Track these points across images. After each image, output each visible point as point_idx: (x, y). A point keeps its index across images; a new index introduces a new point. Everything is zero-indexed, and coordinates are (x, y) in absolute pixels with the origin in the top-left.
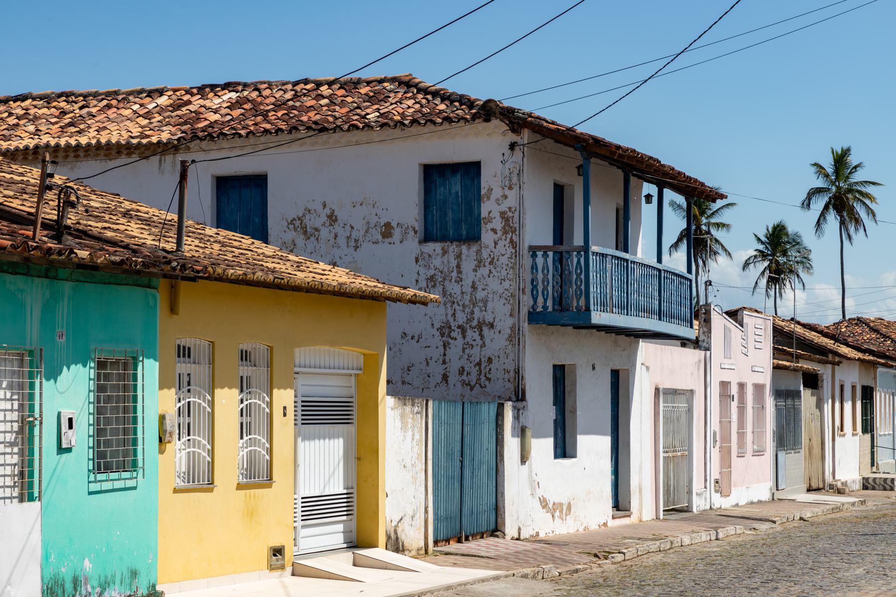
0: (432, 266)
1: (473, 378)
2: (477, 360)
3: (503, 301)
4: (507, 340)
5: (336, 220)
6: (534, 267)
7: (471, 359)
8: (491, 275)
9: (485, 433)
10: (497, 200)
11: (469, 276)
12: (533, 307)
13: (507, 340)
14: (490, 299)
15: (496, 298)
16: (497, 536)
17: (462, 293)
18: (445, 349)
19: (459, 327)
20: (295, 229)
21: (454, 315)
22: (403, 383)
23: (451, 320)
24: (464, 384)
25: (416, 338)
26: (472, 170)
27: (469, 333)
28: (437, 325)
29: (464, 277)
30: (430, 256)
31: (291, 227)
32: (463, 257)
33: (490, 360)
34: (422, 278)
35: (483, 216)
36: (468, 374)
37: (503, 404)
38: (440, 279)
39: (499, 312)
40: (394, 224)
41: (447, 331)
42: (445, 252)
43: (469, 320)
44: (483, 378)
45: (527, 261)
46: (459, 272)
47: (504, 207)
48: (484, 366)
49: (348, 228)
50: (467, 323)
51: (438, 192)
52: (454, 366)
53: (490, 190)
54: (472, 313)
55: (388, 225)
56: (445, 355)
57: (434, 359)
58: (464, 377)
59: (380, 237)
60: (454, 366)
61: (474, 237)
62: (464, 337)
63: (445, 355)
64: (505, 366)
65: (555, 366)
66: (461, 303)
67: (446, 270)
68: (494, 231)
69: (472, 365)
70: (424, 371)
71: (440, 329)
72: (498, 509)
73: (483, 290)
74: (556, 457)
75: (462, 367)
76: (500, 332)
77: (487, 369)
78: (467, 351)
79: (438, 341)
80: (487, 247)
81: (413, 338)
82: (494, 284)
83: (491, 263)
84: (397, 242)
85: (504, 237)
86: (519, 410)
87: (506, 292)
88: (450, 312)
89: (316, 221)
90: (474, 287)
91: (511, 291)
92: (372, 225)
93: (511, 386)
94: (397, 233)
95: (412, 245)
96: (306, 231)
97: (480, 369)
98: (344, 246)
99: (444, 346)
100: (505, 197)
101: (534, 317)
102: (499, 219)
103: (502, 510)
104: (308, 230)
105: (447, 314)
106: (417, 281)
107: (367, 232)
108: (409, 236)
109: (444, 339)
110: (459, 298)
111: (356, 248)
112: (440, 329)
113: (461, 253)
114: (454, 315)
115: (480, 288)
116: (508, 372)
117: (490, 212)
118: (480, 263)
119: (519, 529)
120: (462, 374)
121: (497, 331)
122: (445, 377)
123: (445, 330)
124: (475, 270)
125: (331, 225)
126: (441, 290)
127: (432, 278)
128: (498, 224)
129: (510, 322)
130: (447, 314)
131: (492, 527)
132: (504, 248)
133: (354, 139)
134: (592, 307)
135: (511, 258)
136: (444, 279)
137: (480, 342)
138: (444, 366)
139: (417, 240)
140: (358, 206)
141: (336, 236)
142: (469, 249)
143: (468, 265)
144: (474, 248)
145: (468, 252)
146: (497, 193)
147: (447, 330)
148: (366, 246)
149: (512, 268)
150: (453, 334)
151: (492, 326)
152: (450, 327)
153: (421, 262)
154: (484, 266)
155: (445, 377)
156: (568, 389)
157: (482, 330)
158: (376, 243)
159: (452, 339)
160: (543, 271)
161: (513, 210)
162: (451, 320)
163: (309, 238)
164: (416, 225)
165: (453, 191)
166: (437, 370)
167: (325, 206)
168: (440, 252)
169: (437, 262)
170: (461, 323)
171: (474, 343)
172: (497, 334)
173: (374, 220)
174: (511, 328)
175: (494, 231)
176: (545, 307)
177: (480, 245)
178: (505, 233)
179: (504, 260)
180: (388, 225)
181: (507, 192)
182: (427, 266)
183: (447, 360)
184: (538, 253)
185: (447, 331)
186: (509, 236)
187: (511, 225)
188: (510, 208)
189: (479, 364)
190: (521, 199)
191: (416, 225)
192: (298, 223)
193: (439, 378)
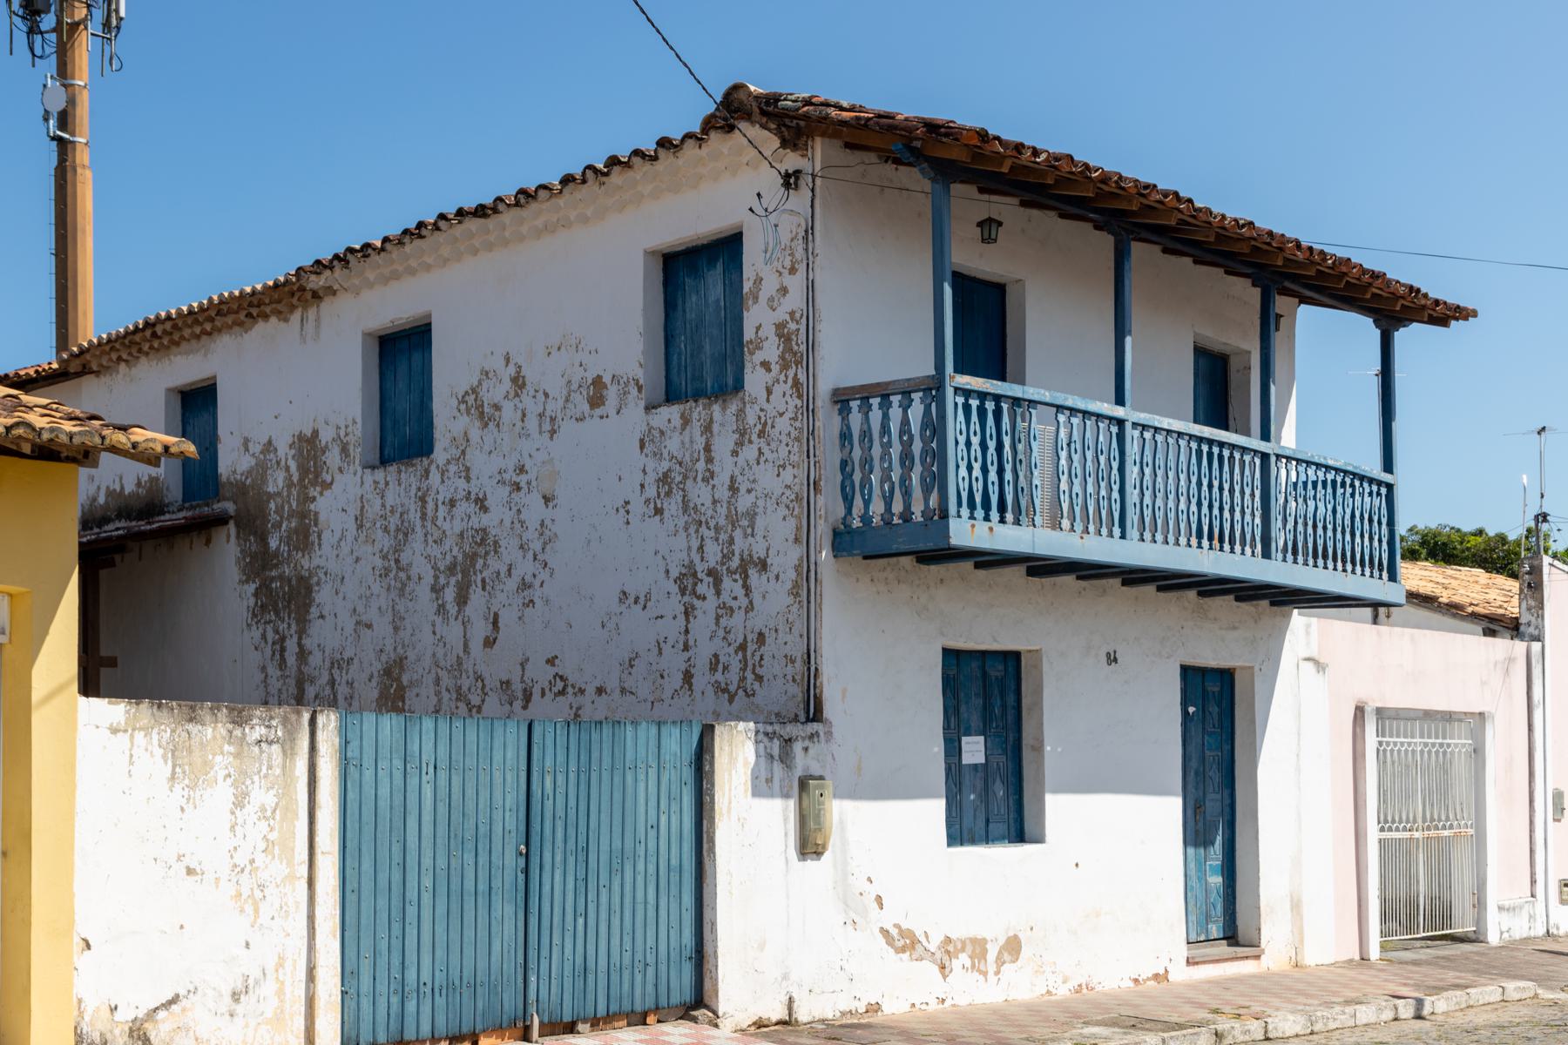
0: (665, 455)
1: (733, 677)
2: (740, 640)
3: (783, 511)
4: (790, 593)
5: (524, 384)
6: (845, 436)
7: (731, 637)
8: (762, 459)
9: (643, 790)
10: (771, 299)
11: (725, 467)
12: (844, 518)
13: (790, 593)
14: (760, 510)
15: (771, 505)
16: (695, 1020)
17: (715, 502)
18: (688, 621)
19: (710, 573)
20: (468, 413)
21: (701, 548)
22: (623, 691)
23: (697, 560)
24: (722, 689)
25: (642, 600)
26: (728, 247)
27: (727, 583)
28: (674, 573)
29: (716, 469)
30: (662, 433)
31: (463, 407)
32: (716, 428)
33: (761, 638)
34: (651, 479)
35: (746, 338)
36: (725, 668)
37: (713, 727)
38: (679, 479)
39: (775, 535)
40: (607, 379)
41: (689, 582)
42: (686, 421)
43: (727, 557)
44: (750, 676)
45: (828, 423)
46: (710, 460)
47: (781, 315)
48: (750, 647)
49: (540, 396)
50: (723, 564)
51: (688, 305)
52: (704, 651)
53: (759, 281)
54: (731, 541)
55: (598, 382)
56: (687, 631)
57: (671, 642)
58: (719, 676)
59: (586, 407)
60: (704, 651)
61: (729, 386)
62: (718, 593)
63: (687, 631)
64: (787, 650)
65: (952, 656)
66: (712, 524)
67: (687, 458)
68: (766, 365)
69: (731, 650)
70: (654, 667)
71: (679, 580)
72: (700, 957)
73: (749, 491)
74: (949, 845)
75: (716, 656)
76: (777, 577)
77: (757, 658)
78: (723, 621)
79: (675, 605)
80: (754, 402)
81: (636, 601)
82: (767, 480)
83: (761, 434)
84: (612, 413)
85: (782, 378)
87: (788, 492)
88: (695, 544)
89: (496, 392)
90: (733, 489)
91: (796, 489)
92: (575, 386)
93: (796, 691)
94: (612, 393)
95: (635, 410)
96: (482, 413)
97: (745, 657)
98: (535, 435)
99: (686, 613)
100: (784, 291)
101: (844, 541)
102: (773, 339)
103: (711, 959)
104: (486, 410)
105: (689, 548)
106: (642, 486)
107: (567, 400)
108: (630, 397)
109: (686, 598)
110: (710, 513)
111: (553, 432)
112: (679, 580)
113: (711, 421)
114: (701, 548)
115: (743, 489)
116: (793, 662)
117: (758, 328)
118: (742, 432)
119: (791, 1000)
120: (716, 670)
121: (772, 576)
122: (688, 677)
123: (687, 581)
124: (735, 453)
125: (517, 395)
126: (680, 500)
127: (665, 479)
128: (771, 351)
129: (796, 553)
130: (689, 548)
131: (688, 996)
132: (784, 401)
133: (539, 222)
134: (952, 509)
135: (795, 419)
136: (685, 477)
137: (744, 602)
138: (686, 655)
139: (642, 404)
140: (554, 351)
141: (524, 415)
142: (724, 409)
143: (723, 443)
144: (733, 407)
145: (722, 415)
146: (769, 287)
147: (691, 580)
148: (567, 428)
149: (797, 439)
150: (701, 589)
151: (763, 565)
152: (695, 575)
153: (649, 449)
154: (750, 442)
155: (688, 677)
156: (1025, 702)
157: (747, 576)
158: (580, 419)
159: (698, 597)
160: (861, 441)
161: (798, 315)
162: (697, 560)
163: (486, 425)
164: (640, 374)
165: (712, 299)
166: (674, 662)
167: (508, 360)
168: (677, 422)
169: (673, 444)
170: (712, 564)
171: (735, 604)
172: (773, 581)
173: (577, 375)
174: (797, 568)
175: (766, 365)
176: (866, 519)
177: (743, 399)
178: (785, 367)
179: (783, 424)
180: (598, 382)
181: (788, 280)
182: (658, 455)
183: (691, 643)
184: (852, 404)
185: (689, 582)
186: (791, 373)
187: (798, 350)
188: (792, 314)
189: (743, 647)
190: (811, 287)
191: (640, 374)
192: (471, 399)
193: (678, 679)
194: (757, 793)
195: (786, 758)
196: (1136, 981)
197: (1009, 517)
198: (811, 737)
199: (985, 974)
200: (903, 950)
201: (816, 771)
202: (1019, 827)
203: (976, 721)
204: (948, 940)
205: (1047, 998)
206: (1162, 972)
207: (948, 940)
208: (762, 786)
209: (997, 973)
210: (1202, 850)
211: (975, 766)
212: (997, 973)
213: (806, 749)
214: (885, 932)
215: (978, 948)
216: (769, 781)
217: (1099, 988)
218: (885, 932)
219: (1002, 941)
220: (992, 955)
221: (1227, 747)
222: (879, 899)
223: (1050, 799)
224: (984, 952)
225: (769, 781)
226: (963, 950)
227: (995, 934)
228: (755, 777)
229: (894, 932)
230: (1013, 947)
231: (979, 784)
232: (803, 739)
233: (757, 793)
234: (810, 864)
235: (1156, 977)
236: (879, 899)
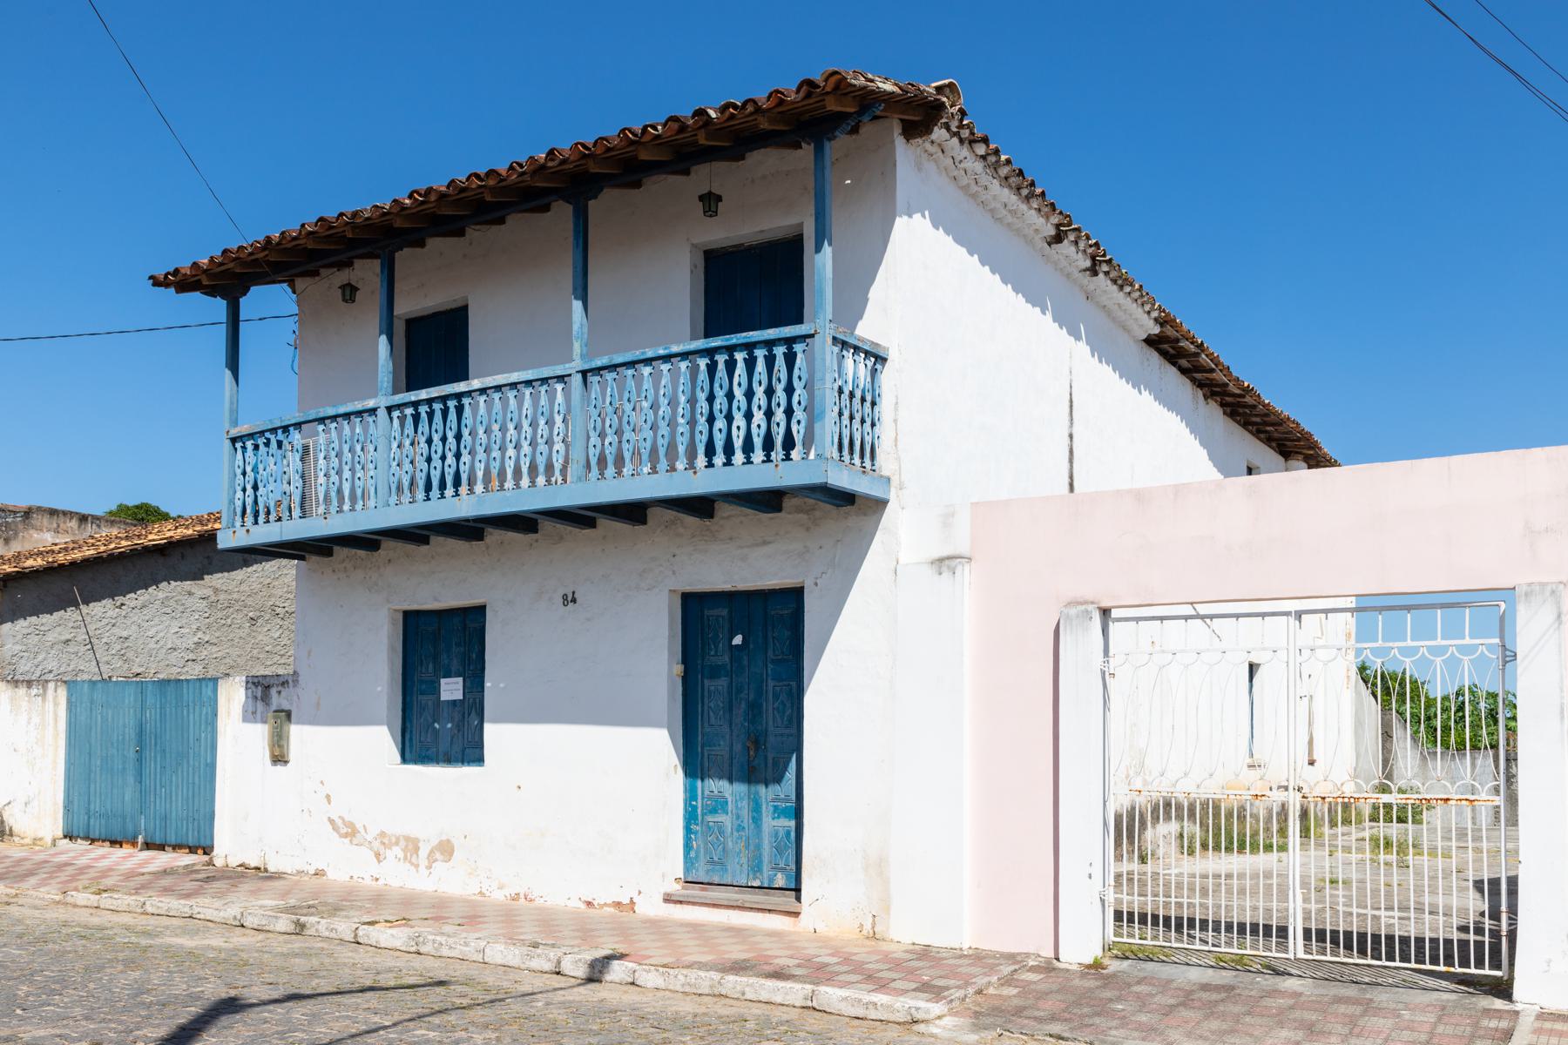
86: (268, 687)
194: (245, 720)
195: (265, 698)
196: (589, 904)
197: (261, 519)
199: (417, 866)
200: (346, 835)
201: (286, 706)
202: (470, 751)
204: (383, 834)
205: (478, 898)
206: (626, 901)
207: (383, 834)
208: (250, 716)
209: (429, 867)
210: (762, 789)
211: (455, 701)
212: (429, 867)
214: (331, 821)
215: (411, 846)
216: (254, 713)
217: (539, 902)
218: (331, 821)
219: (435, 842)
220: (424, 852)
222: (328, 797)
223: (488, 727)
224: (417, 849)
225: (254, 713)
226: (397, 843)
227: (429, 836)
228: (245, 711)
229: (339, 822)
230: (446, 849)
231: (457, 717)
233: (245, 720)
234: (279, 768)
235: (618, 904)
236: (328, 797)
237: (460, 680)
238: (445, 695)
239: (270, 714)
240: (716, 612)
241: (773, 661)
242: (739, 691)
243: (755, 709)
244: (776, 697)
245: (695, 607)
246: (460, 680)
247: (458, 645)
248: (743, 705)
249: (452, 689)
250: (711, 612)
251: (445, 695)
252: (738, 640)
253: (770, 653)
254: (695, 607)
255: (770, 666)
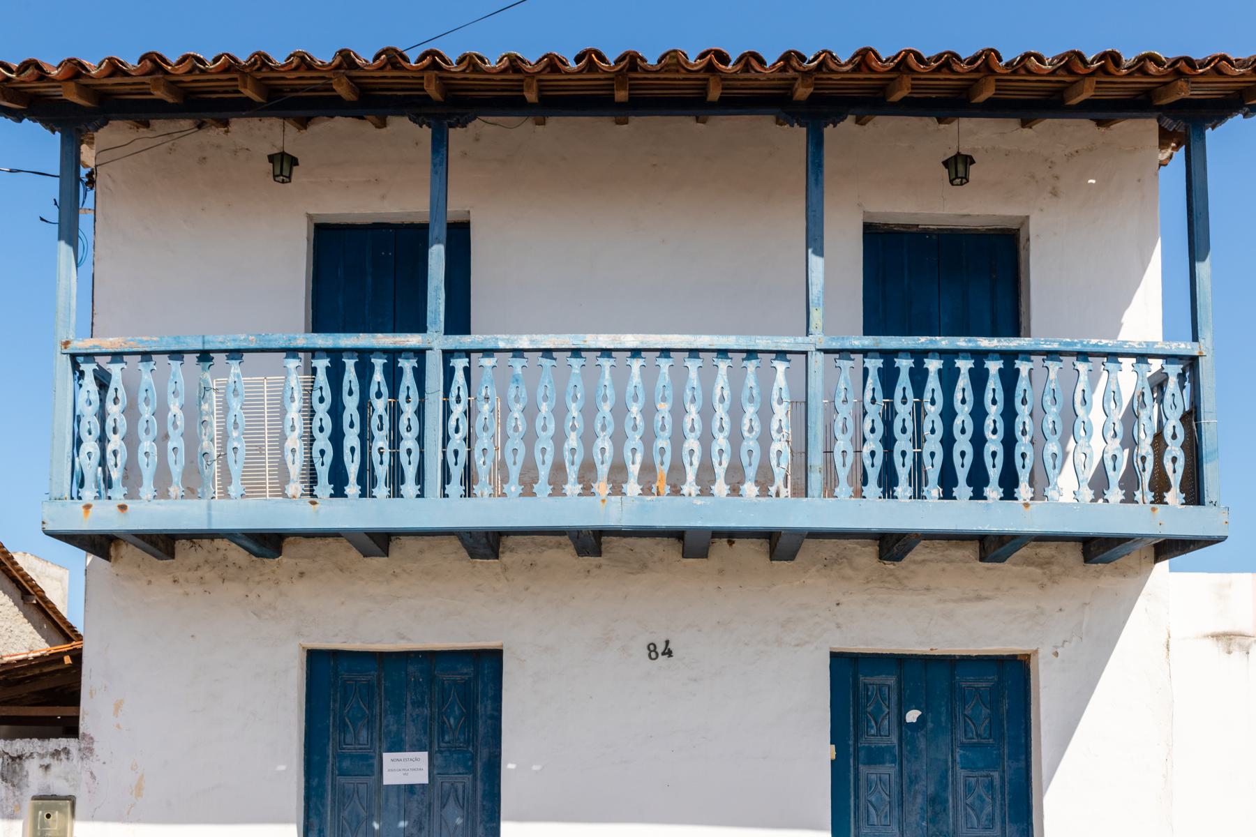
198: (56, 754)
201: (61, 788)
203: (411, 732)
211: (411, 789)
213: (47, 767)
221: (1022, 764)
232: (42, 756)
237: (424, 756)
238: (389, 778)
239: (28, 804)
240: (877, 680)
241: (963, 746)
242: (913, 781)
243: (936, 803)
244: (969, 789)
245: (846, 667)
246: (424, 756)
247: (418, 704)
248: (920, 799)
249: (405, 768)
250: (868, 680)
251: (389, 778)
252: (912, 716)
253: (960, 736)
254: (846, 667)
255: (959, 752)
